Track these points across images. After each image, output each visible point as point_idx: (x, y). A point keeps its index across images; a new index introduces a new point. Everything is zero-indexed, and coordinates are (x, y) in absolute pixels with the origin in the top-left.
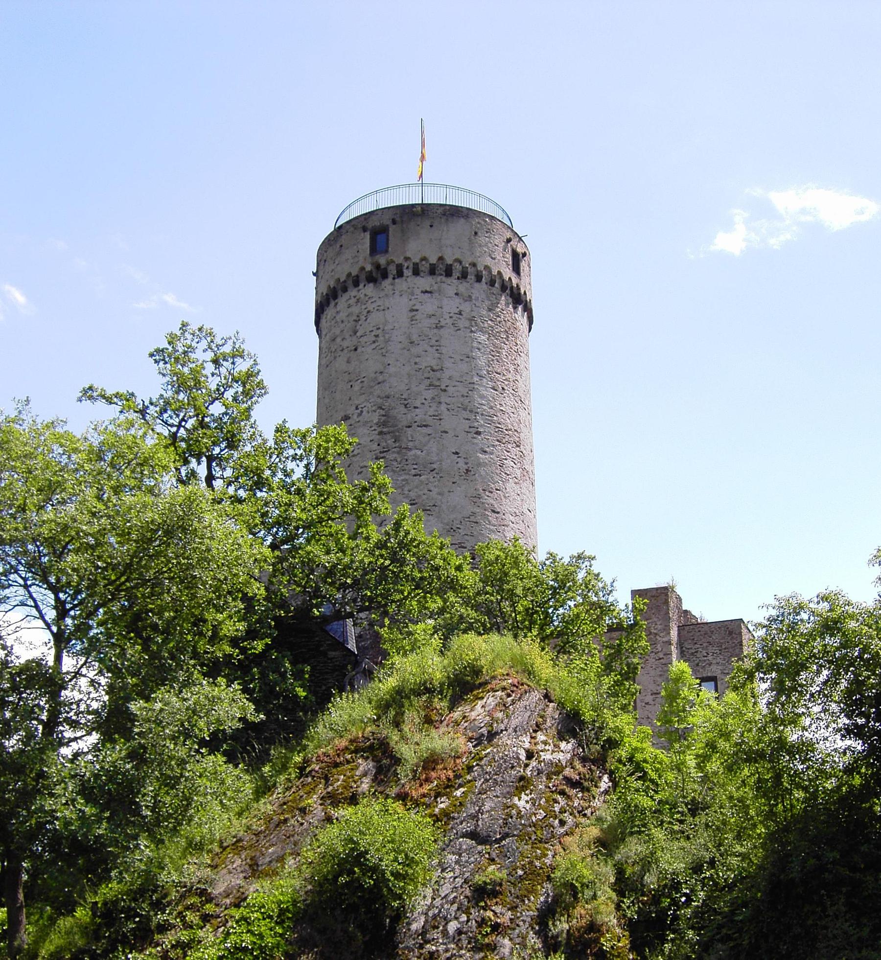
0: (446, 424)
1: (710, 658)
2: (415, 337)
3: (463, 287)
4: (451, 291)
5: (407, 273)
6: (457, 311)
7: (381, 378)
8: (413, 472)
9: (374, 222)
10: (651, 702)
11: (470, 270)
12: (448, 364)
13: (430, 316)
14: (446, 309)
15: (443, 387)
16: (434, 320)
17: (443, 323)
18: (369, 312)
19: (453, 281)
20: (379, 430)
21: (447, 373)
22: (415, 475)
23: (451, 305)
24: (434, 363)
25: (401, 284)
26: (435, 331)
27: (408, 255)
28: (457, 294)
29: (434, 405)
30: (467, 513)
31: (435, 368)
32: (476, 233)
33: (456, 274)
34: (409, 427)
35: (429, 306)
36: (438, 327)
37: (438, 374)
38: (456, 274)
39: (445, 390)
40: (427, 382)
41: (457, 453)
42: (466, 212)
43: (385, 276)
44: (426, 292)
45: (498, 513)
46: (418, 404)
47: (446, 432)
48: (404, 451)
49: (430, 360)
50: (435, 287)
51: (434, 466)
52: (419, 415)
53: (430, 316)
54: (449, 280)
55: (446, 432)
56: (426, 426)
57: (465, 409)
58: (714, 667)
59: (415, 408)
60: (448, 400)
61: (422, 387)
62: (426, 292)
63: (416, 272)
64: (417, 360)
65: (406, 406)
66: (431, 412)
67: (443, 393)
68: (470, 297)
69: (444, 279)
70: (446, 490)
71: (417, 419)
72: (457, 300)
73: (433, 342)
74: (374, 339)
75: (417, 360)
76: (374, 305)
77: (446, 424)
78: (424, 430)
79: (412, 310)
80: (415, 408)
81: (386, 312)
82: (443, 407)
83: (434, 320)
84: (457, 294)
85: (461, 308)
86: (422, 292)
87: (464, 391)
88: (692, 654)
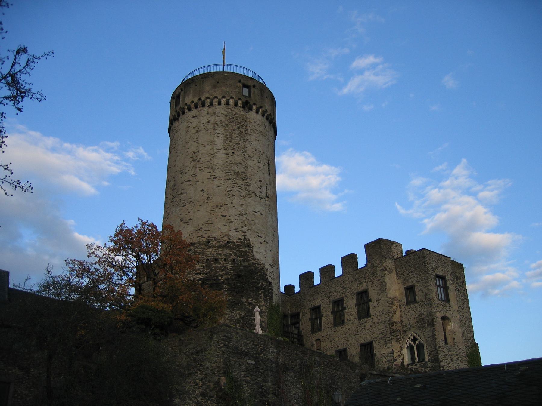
0: (198, 178)
1: (410, 275)
2: (188, 140)
3: (211, 110)
5: (186, 111)
6: (207, 121)
8: (183, 205)
10: (377, 306)
12: (201, 148)
13: (194, 128)
14: (202, 122)
15: (198, 160)
16: (196, 129)
19: (206, 107)
21: (201, 152)
24: (194, 149)
25: (185, 116)
26: (197, 134)
27: (186, 102)
29: (193, 170)
30: (206, 220)
32: (218, 82)
34: (182, 183)
35: (195, 122)
36: (197, 132)
37: (196, 154)
39: (199, 161)
40: (191, 159)
41: (203, 190)
42: (212, 74)
44: (194, 117)
45: (226, 216)
46: (186, 171)
47: (198, 181)
50: (198, 113)
51: (191, 200)
52: (187, 176)
53: (194, 128)
54: (204, 109)
55: (198, 181)
56: (189, 181)
57: (208, 168)
58: (412, 280)
60: (200, 165)
61: (189, 162)
62: (194, 117)
63: (189, 109)
64: (188, 150)
65: (182, 173)
66: (192, 173)
67: (198, 163)
68: (215, 113)
69: (202, 108)
70: (196, 210)
72: (208, 116)
73: (195, 140)
75: (188, 150)
77: (198, 178)
78: (188, 183)
82: (198, 170)
83: (196, 129)
84: (207, 114)
85: (209, 119)
86: (193, 117)
87: (208, 158)
88: (402, 274)
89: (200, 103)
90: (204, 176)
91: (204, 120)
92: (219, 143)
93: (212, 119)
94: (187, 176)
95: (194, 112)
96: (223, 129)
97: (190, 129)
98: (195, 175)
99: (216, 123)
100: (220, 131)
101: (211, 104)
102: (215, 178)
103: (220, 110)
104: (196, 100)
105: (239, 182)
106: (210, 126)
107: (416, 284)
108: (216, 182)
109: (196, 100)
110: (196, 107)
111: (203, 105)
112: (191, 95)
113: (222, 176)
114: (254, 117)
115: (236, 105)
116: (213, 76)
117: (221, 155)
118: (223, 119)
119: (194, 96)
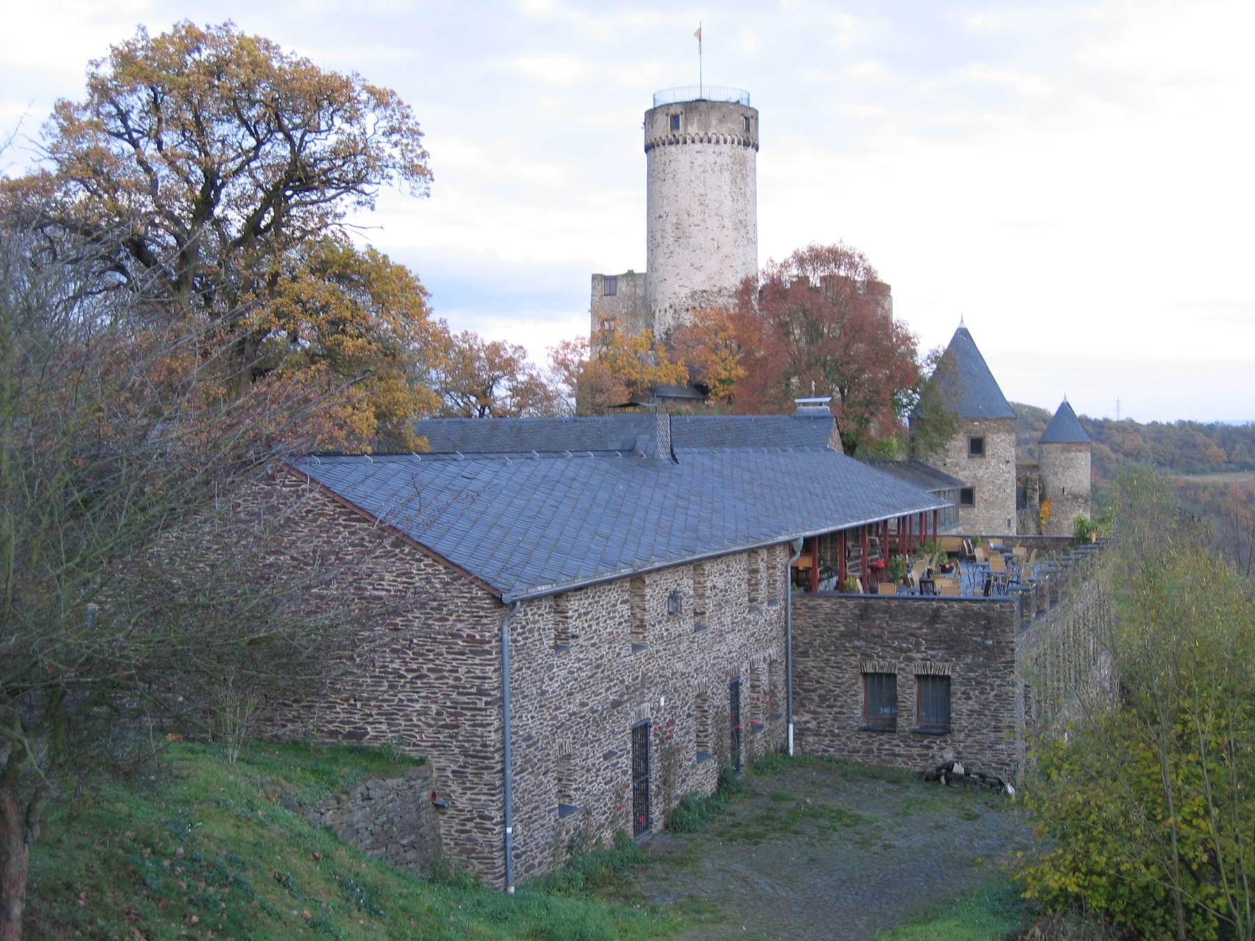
0: (708, 225)
3: (717, 148)
4: (711, 151)
5: (689, 141)
9: (673, 111)
11: (721, 138)
12: (709, 192)
19: (712, 145)
23: (711, 158)
33: (713, 141)
35: (700, 160)
38: (713, 141)
43: (678, 142)
49: (700, 190)
52: (695, 220)
63: (693, 142)
77: (708, 225)
89: (706, 139)
90: (712, 223)
91: (711, 158)
92: (726, 188)
93: (719, 160)
94: (696, 219)
95: (698, 146)
97: (695, 166)
99: (722, 165)
100: (727, 174)
101: (718, 142)
103: (726, 148)
104: (702, 134)
105: (742, 231)
106: (717, 168)
108: (725, 232)
109: (702, 134)
111: (710, 141)
112: (695, 125)
113: (729, 224)
114: (750, 150)
115: (739, 143)
116: (719, 109)
117: (728, 202)
118: (729, 161)
119: (699, 128)
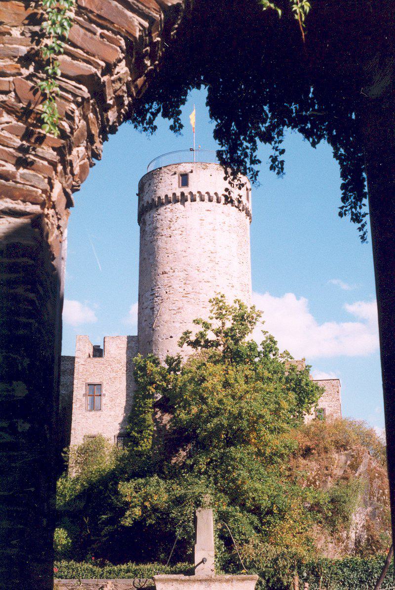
5: (198, 199)
7: (185, 254)
8: (202, 306)
17: (216, 228)
18: (177, 218)
19: (221, 205)
20: (184, 282)
22: (203, 308)
28: (223, 213)
31: (213, 251)
34: (200, 282)
37: (214, 255)
44: (208, 210)
46: (204, 270)
47: (218, 286)
48: (198, 294)
58: (324, 403)
59: (203, 272)
65: (198, 270)
67: (216, 265)
68: (229, 214)
71: (204, 278)
74: (181, 233)
76: (181, 214)
78: (207, 284)
79: (201, 220)
80: (203, 272)
81: (188, 219)
82: (217, 273)
95: (206, 204)
96: (236, 235)
98: (214, 277)
102: (233, 287)
107: (327, 408)
110: (210, 200)
